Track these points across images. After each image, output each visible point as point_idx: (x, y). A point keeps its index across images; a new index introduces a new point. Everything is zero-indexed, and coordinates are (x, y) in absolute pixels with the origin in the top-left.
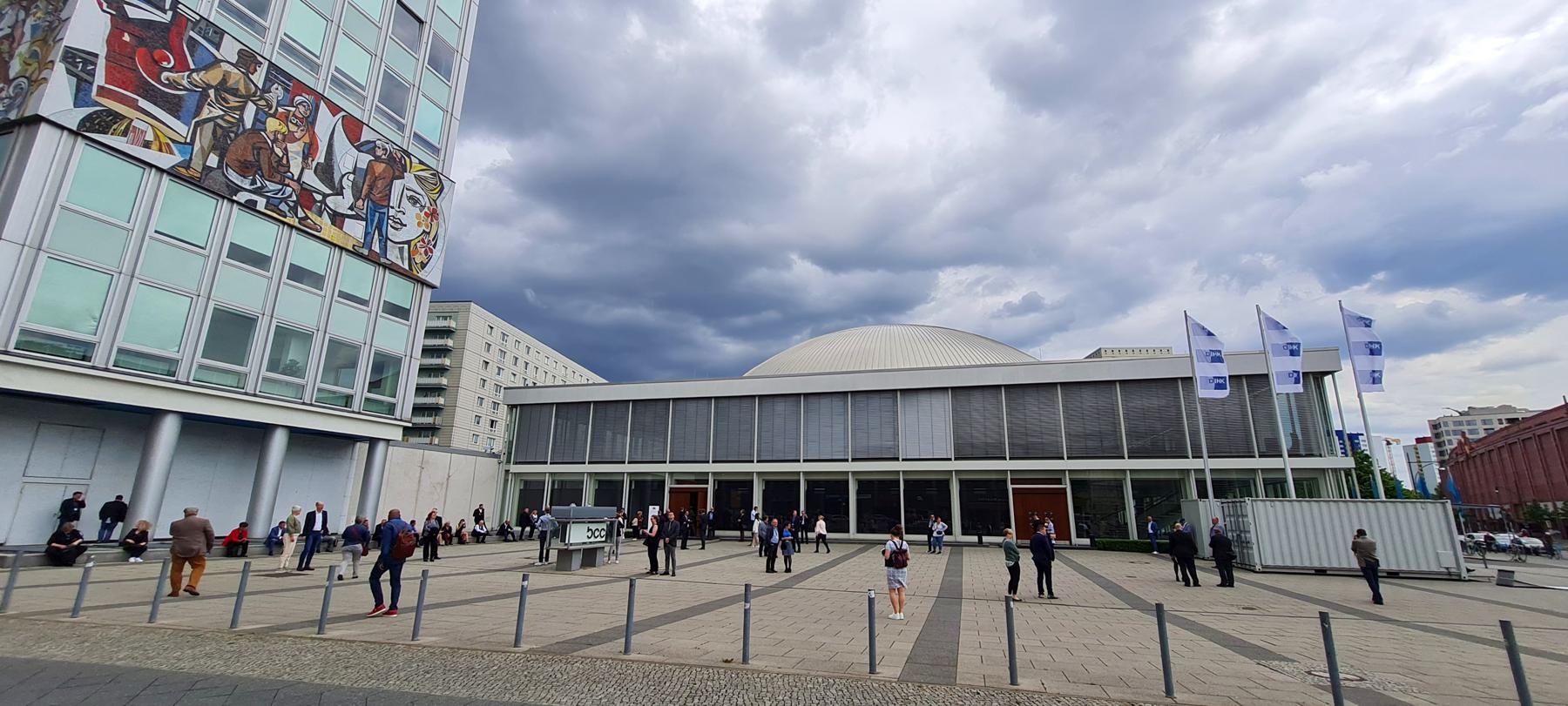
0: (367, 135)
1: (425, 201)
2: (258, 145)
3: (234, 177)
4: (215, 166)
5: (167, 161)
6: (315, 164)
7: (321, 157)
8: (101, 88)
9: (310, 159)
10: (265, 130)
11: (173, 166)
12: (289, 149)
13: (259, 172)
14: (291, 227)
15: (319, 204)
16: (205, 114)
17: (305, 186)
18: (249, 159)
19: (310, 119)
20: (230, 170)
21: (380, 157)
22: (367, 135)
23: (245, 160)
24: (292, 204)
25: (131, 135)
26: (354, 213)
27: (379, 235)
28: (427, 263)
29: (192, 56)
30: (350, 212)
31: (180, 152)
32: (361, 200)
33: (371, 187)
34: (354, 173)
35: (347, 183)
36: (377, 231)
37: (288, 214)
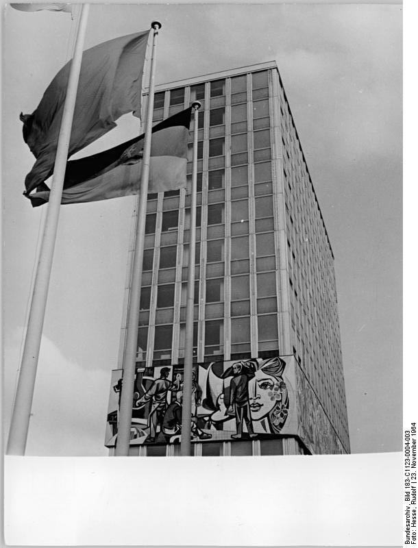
3: (168, 432)
6: (202, 401)
7: (204, 396)
10: (176, 400)
16: (153, 410)
20: (166, 430)
24: (194, 430)
27: (246, 421)
29: (145, 387)
33: (235, 395)
34: (223, 393)
35: (221, 402)
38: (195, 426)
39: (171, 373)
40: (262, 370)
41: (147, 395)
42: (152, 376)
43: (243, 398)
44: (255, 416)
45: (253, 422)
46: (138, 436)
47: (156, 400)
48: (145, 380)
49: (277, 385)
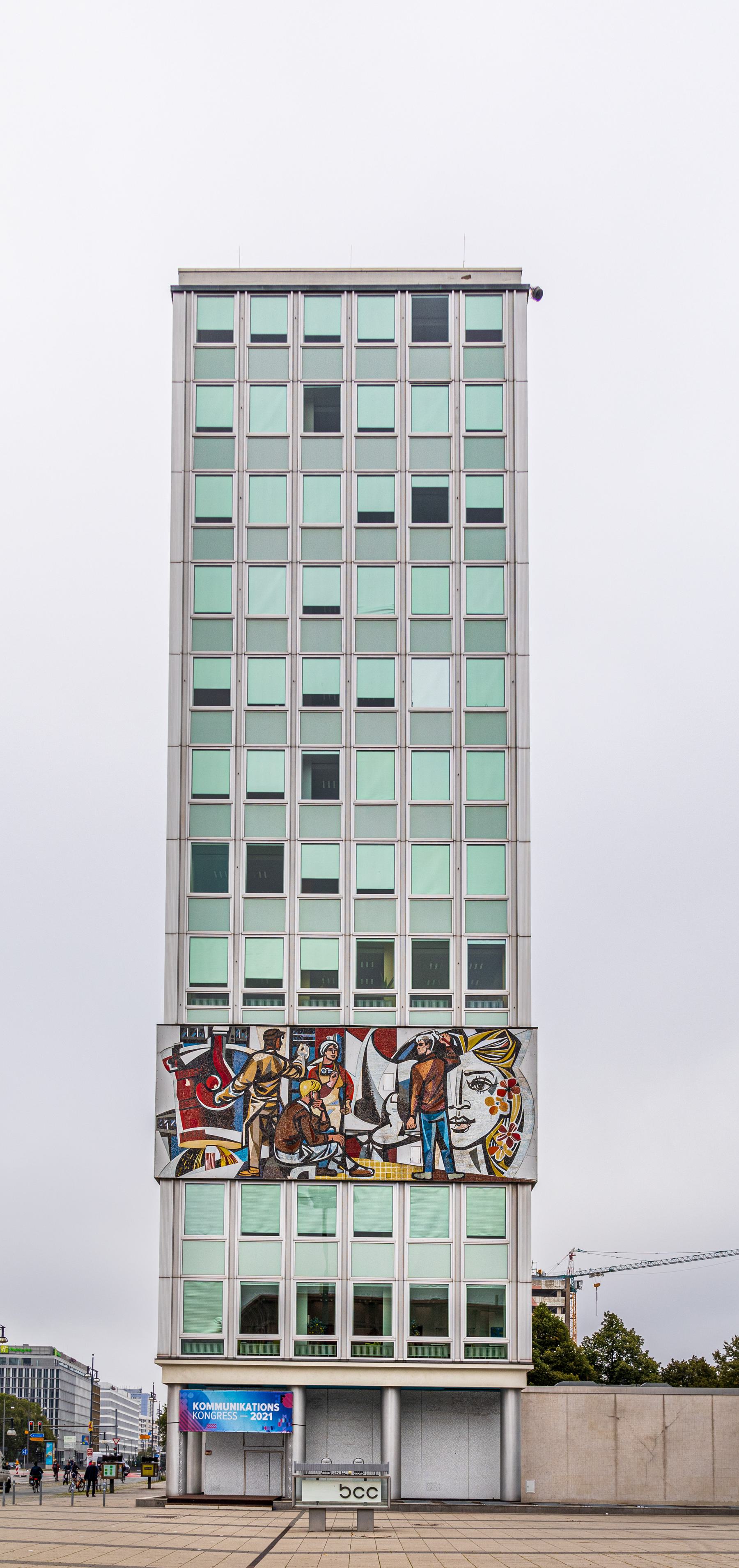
0: (403, 1038)
2: (297, 1116)
3: (284, 1158)
4: (268, 1157)
5: (231, 1171)
7: (358, 1095)
8: (182, 1135)
9: (348, 1102)
10: (300, 1098)
11: (239, 1173)
12: (325, 1104)
13: (304, 1142)
14: (345, 1182)
15: (366, 1146)
16: (251, 1113)
17: (348, 1133)
18: (293, 1134)
19: (340, 1060)
20: (280, 1154)
21: (424, 1055)
22: (403, 1038)
23: (290, 1137)
24: (339, 1159)
25: (206, 1162)
26: (406, 1137)
27: (441, 1149)
28: (514, 1155)
29: (231, 1066)
30: (401, 1138)
31: (241, 1158)
32: (411, 1118)
33: (420, 1097)
34: (397, 1090)
35: (392, 1108)
36: (437, 1145)
37: (338, 1171)
38: (340, 1151)
39: (286, 1041)
40: (475, 1052)
41: (237, 1083)
43: (436, 1104)
45: (455, 1152)
46: (223, 1163)
47: (257, 1093)
48: (230, 1052)
49: (502, 1084)
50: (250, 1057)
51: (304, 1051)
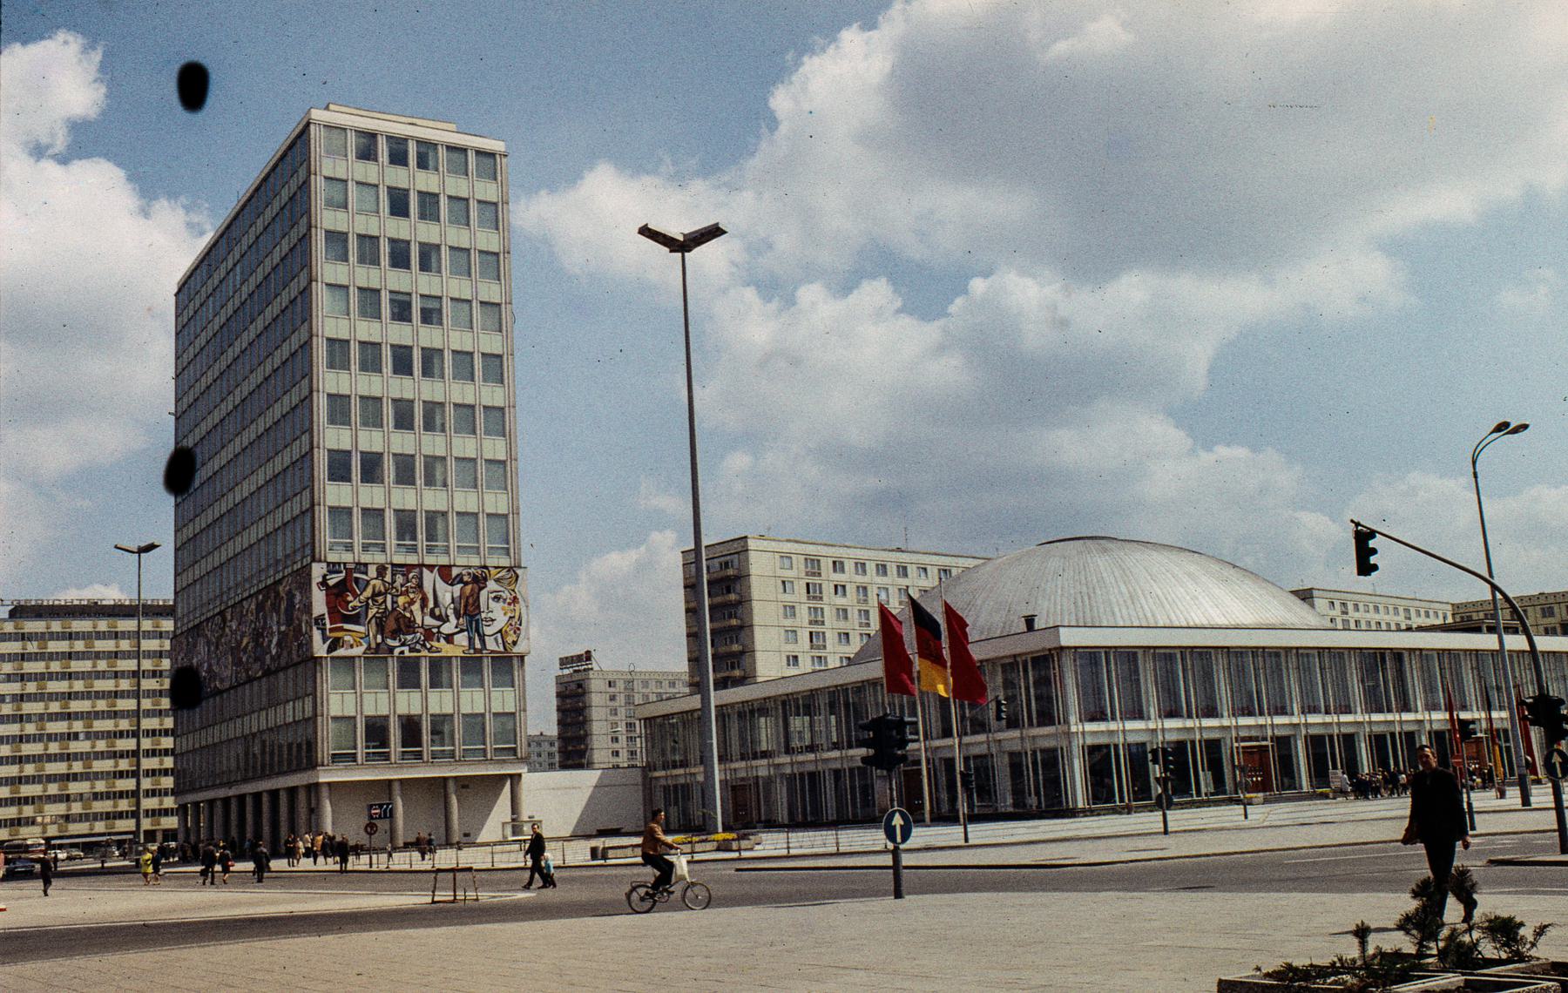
0: (455, 572)
1: (506, 595)
3: (390, 642)
7: (431, 604)
16: (370, 616)
22: (455, 572)
33: (466, 606)
34: (453, 602)
35: (450, 612)
42: (366, 573)
44: (488, 631)
48: (357, 579)
50: (368, 582)
51: (400, 579)
